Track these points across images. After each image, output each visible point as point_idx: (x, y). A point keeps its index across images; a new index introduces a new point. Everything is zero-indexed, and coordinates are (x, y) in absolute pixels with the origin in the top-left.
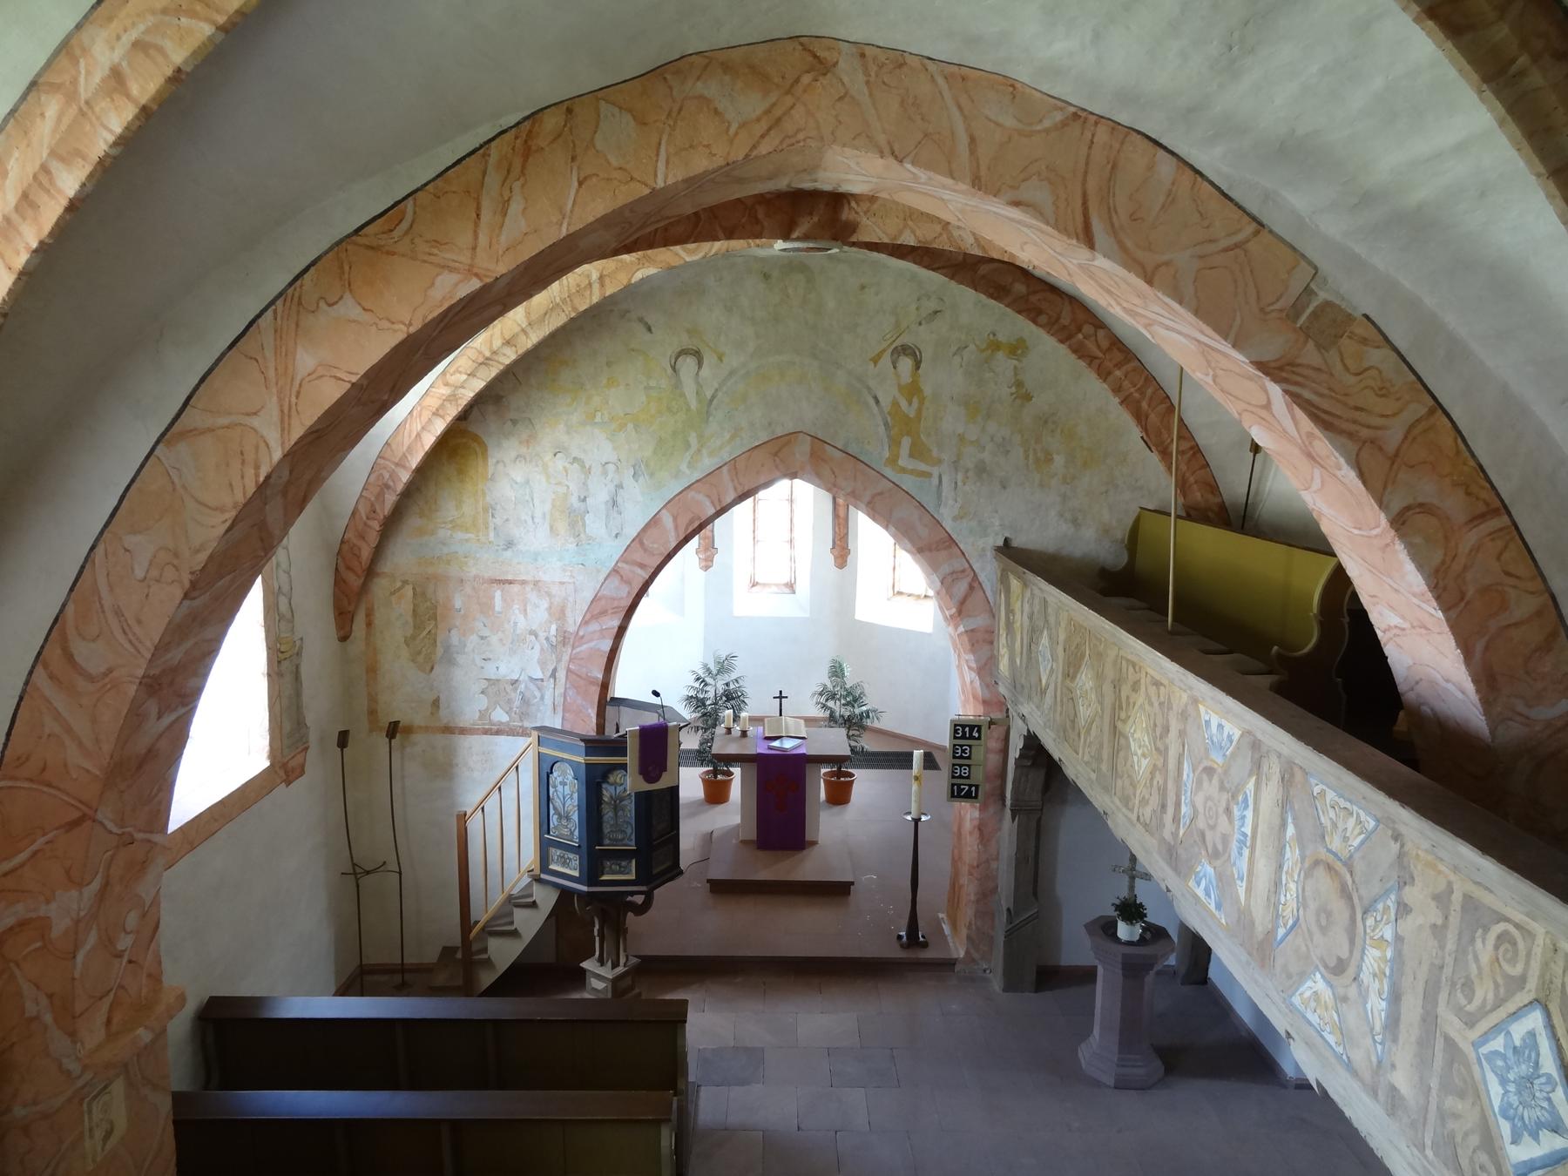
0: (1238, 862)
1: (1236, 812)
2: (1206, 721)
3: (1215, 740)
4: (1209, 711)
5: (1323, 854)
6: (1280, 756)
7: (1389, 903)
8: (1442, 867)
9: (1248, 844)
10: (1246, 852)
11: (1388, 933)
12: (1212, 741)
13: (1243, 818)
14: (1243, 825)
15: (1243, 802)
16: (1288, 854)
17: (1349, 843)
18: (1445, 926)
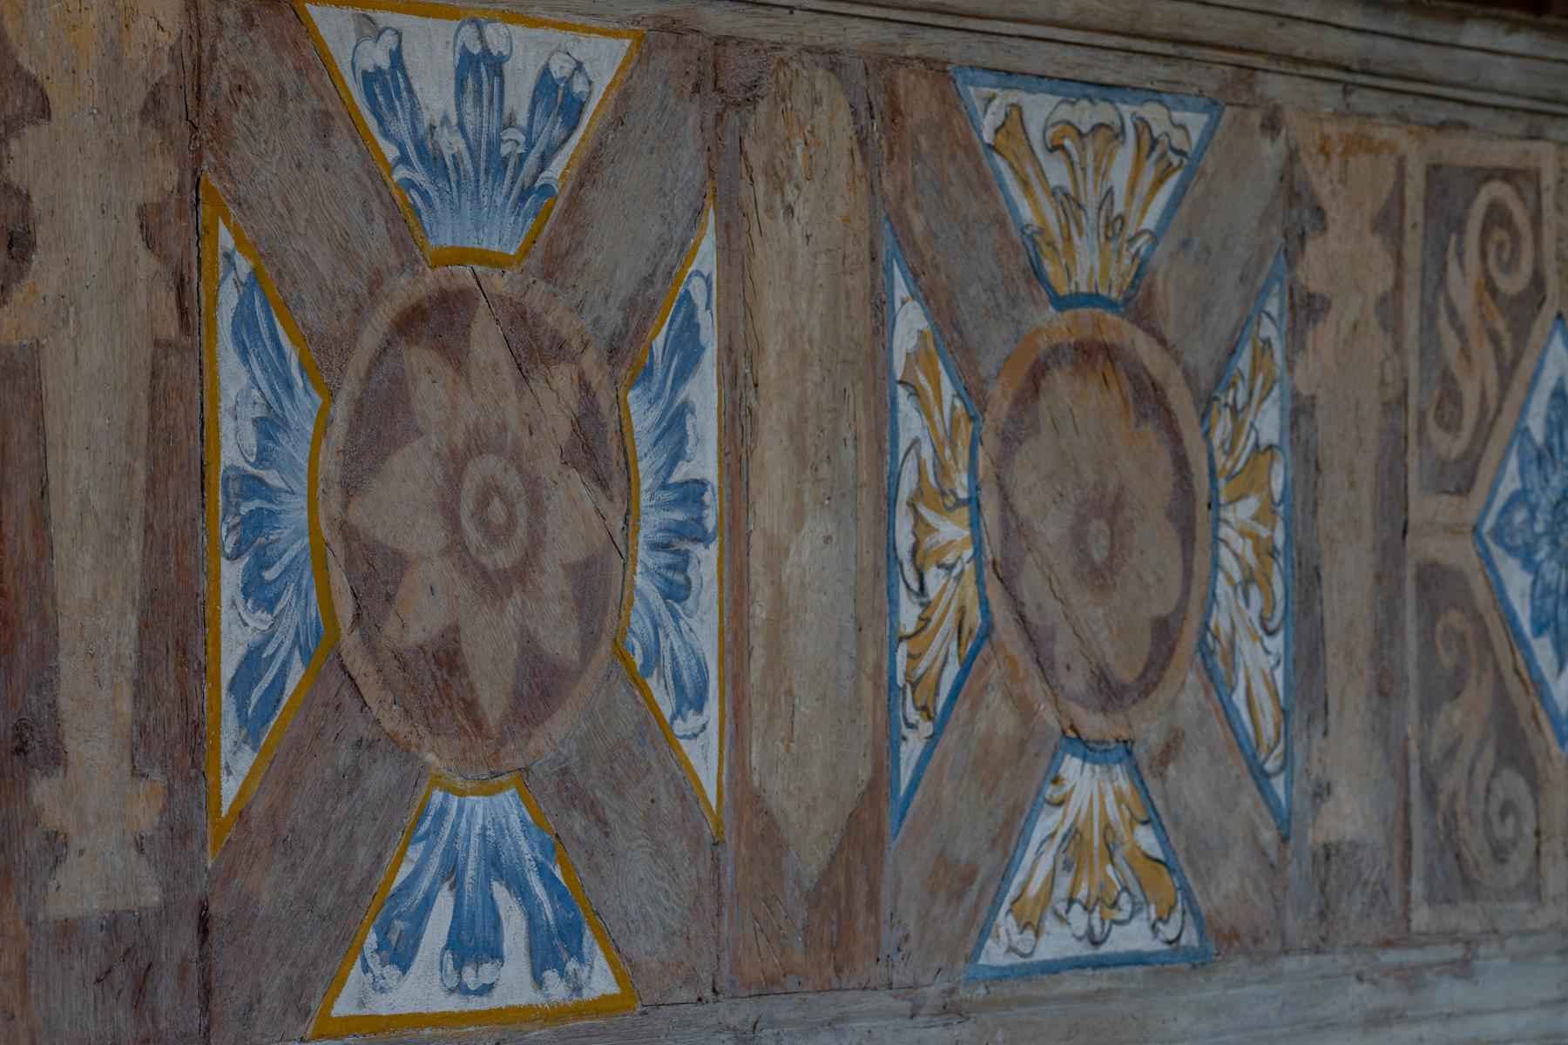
0: (671, 641)
1: (643, 417)
2: (369, 79)
3: (451, 143)
4: (383, 18)
5: (1051, 324)
6: (832, 59)
7: (1268, 330)
8: (1383, 134)
9: (711, 522)
10: (706, 561)
11: (1268, 423)
12: (434, 162)
13: (675, 424)
14: (677, 456)
15: (670, 350)
16: (911, 421)
17: (1131, 231)
18: (1398, 285)
